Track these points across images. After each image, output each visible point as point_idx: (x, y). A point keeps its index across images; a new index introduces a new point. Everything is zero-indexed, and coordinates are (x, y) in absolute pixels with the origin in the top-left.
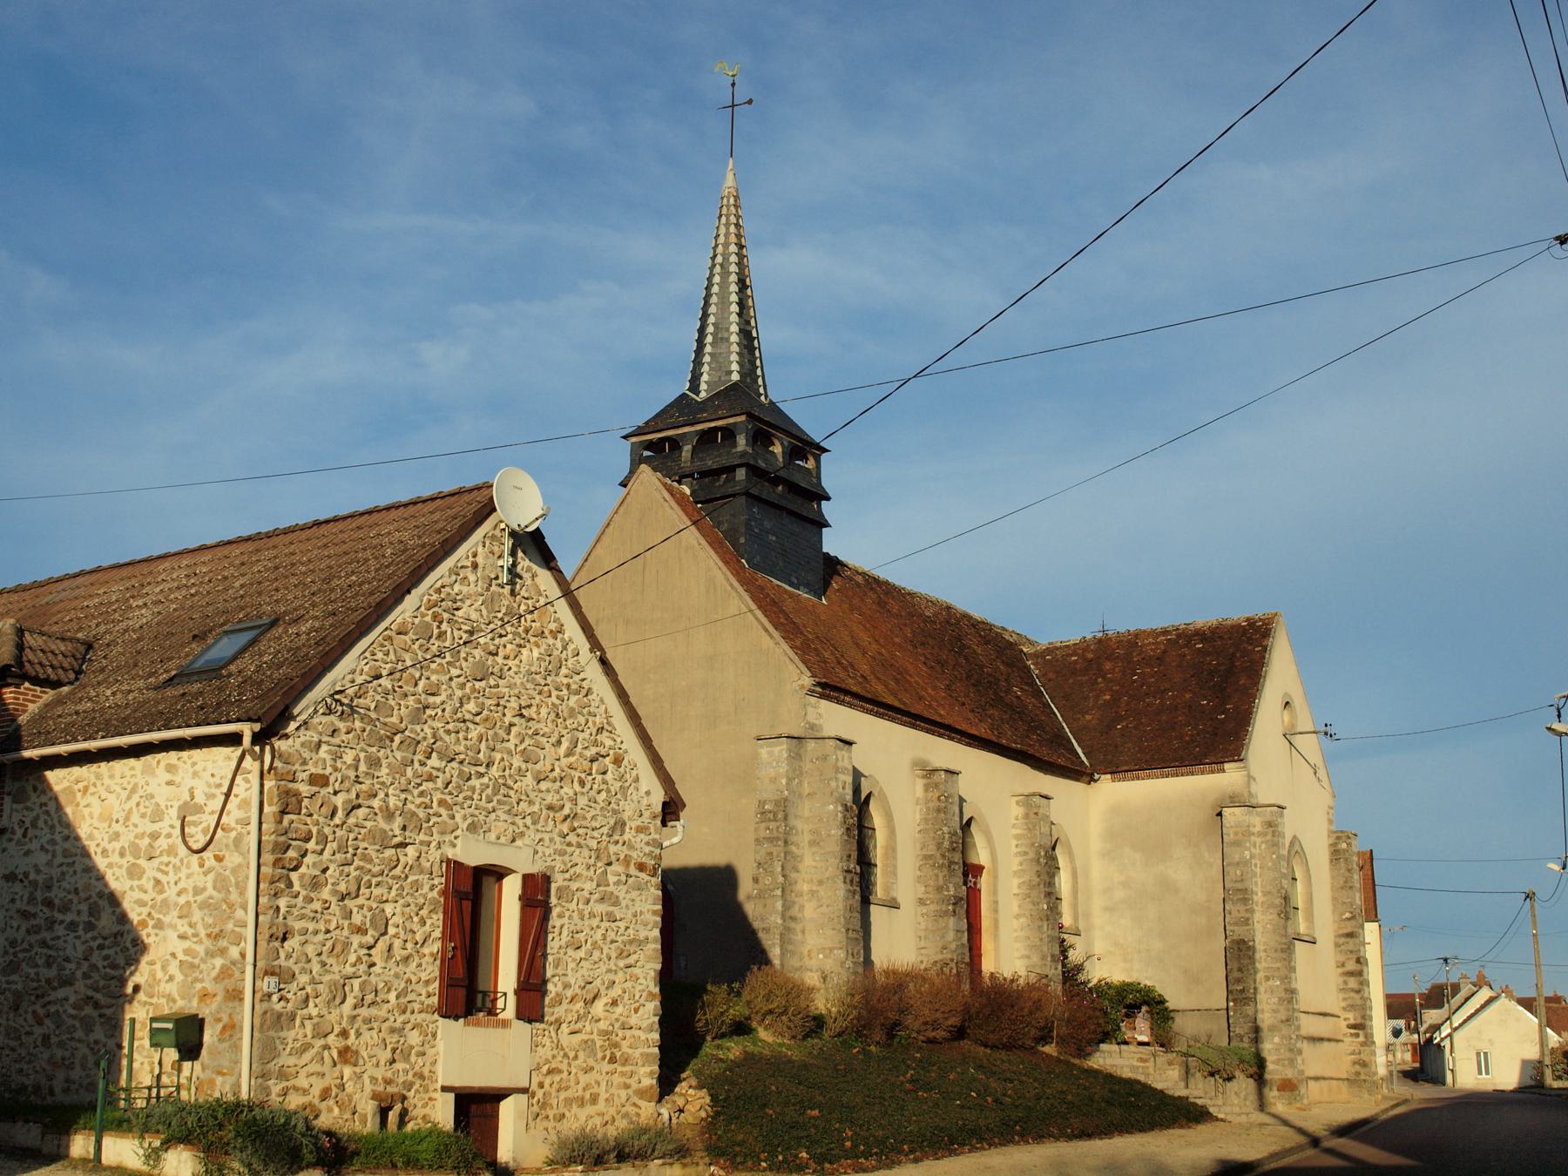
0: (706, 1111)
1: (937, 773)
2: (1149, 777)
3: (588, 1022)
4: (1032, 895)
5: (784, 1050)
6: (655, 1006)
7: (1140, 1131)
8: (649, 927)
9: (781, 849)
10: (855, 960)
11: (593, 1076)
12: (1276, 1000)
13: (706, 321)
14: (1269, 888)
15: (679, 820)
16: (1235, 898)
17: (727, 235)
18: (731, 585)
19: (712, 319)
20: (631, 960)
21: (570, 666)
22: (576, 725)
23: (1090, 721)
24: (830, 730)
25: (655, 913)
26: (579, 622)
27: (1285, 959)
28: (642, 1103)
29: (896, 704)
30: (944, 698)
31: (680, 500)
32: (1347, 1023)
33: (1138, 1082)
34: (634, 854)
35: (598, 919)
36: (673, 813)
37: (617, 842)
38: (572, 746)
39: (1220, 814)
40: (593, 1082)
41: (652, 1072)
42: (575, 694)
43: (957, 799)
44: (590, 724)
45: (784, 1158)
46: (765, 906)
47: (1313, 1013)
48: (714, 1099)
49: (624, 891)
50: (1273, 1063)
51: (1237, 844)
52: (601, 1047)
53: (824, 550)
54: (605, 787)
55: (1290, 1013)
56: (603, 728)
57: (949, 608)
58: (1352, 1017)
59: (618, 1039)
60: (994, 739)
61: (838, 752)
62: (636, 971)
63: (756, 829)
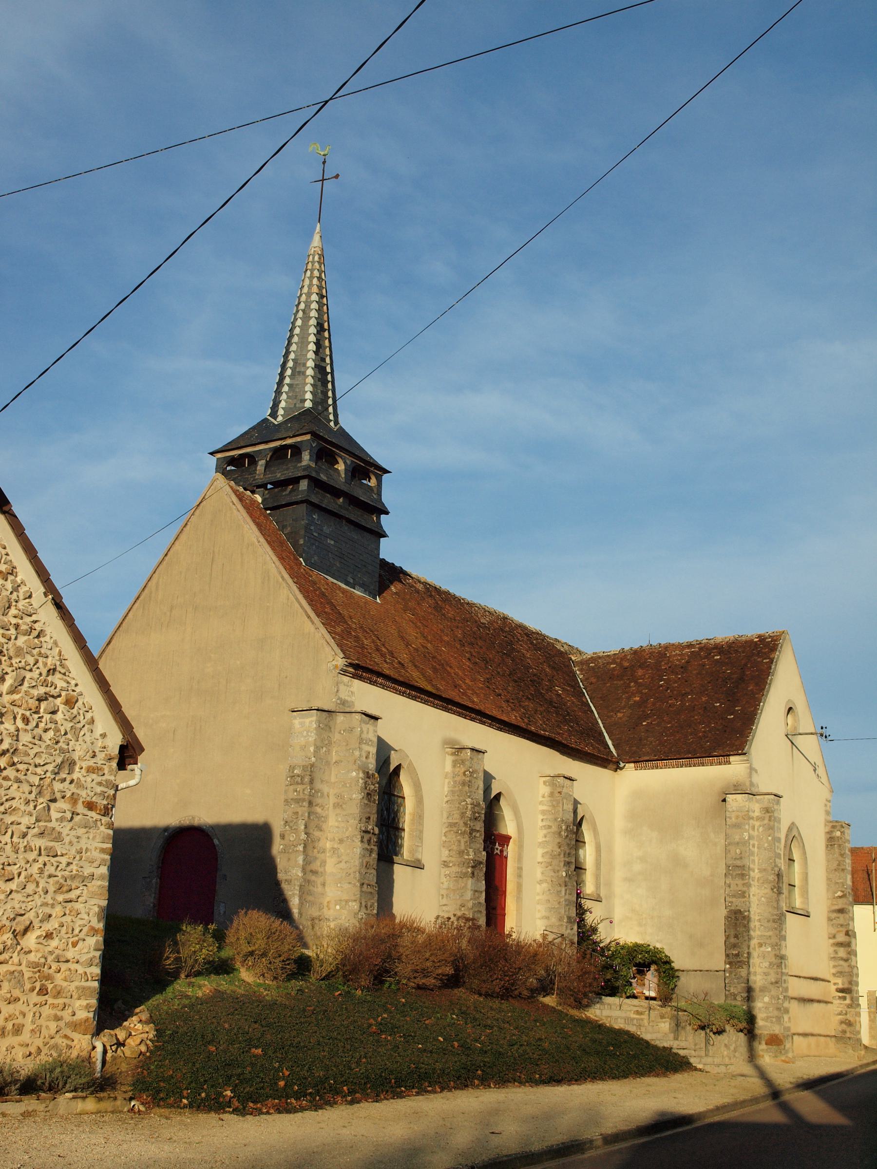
0: (147, 1045)
1: (464, 751)
2: (666, 767)
3: (16, 954)
4: (553, 863)
5: (262, 990)
6: (97, 941)
7: (613, 1078)
8: (96, 864)
9: (305, 809)
10: (368, 912)
11: (19, 1006)
12: (767, 964)
13: (288, 357)
14: (764, 866)
15: (137, 764)
16: (734, 874)
17: (310, 286)
18: (282, 577)
19: (292, 356)
20: (73, 895)
21: (21, 607)
22: (23, 664)
23: (620, 718)
24: (361, 705)
25: (103, 851)
26: (33, 566)
27: (776, 929)
28: (76, 1036)
29: (429, 688)
30: (482, 688)
31: (250, 507)
32: (836, 987)
33: (627, 1033)
34: (83, 793)
35: (37, 852)
36: (130, 757)
37: (64, 780)
38: (16, 684)
39: (724, 800)
40: (17, 1013)
41: (88, 1007)
42: (24, 635)
43: (481, 775)
44: (40, 664)
45: (207, 1095)
46: (289, 859)
47: (805, 978)
48: (159, 1033)
49: (69, 828)
50: (763, 1020)
51: (737, 826)
52: (29, 978)
53: (381, 557)
54: (53, 726)
55: (779, 976)
56: (54, 670)
57: (505, 618)
58: (840, 982)
59: (51, 971)
60: (523, 725)
61: (363, 725)
62: (78, 906)
63: (286, 792)
